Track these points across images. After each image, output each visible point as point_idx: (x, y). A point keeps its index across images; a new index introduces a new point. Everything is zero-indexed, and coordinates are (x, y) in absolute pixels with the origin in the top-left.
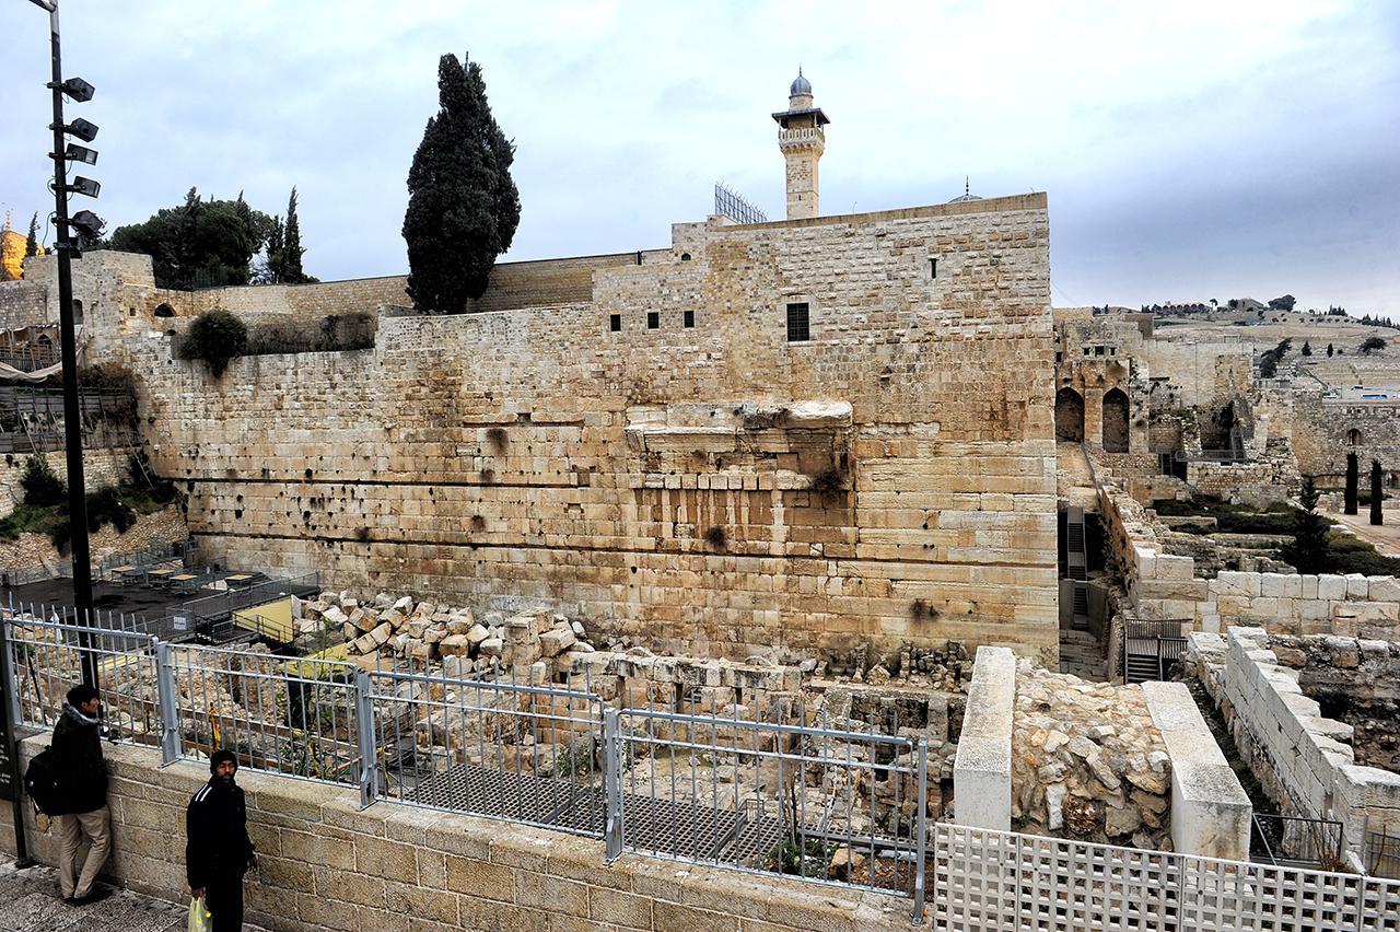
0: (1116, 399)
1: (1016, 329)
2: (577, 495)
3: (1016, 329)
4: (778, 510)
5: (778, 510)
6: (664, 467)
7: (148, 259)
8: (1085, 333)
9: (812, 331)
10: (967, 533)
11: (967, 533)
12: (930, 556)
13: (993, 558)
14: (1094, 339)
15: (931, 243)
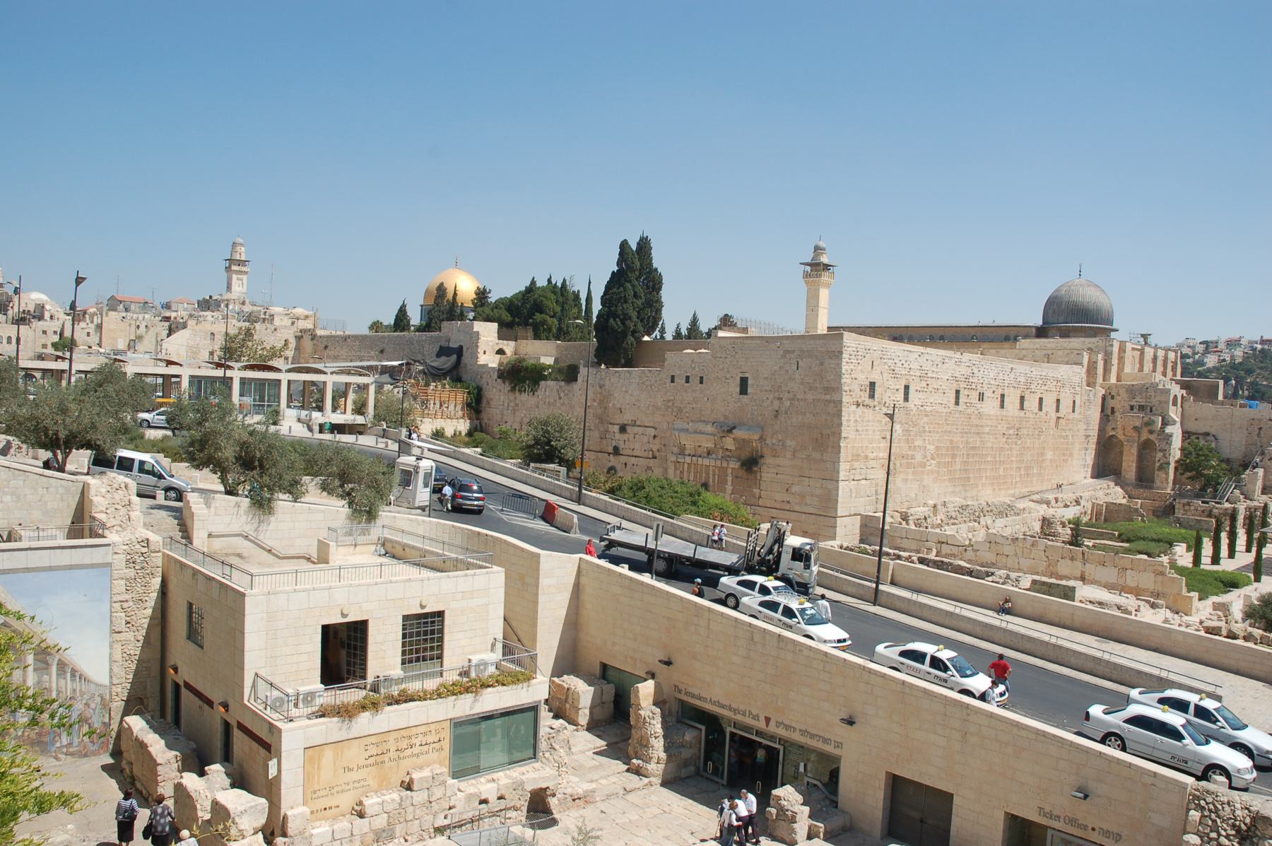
0: (1146, 448)
1: (828, 397)
2: (651, 463)
3: (828, 397)
4: (730, 478)
5: (730, 478)
6: (687, 452)
7: (496, 325)
8: (1132, 391)
9: (749, 390)
10: (803, 496)
11: (803, 496)
12: (787, 507)
13: (812, 511)
14: (1138, 399)
15: (797, 353)
